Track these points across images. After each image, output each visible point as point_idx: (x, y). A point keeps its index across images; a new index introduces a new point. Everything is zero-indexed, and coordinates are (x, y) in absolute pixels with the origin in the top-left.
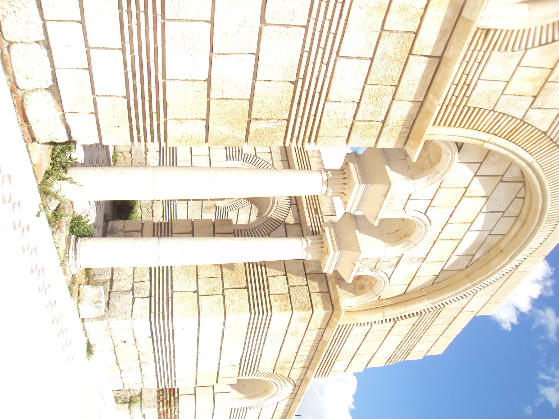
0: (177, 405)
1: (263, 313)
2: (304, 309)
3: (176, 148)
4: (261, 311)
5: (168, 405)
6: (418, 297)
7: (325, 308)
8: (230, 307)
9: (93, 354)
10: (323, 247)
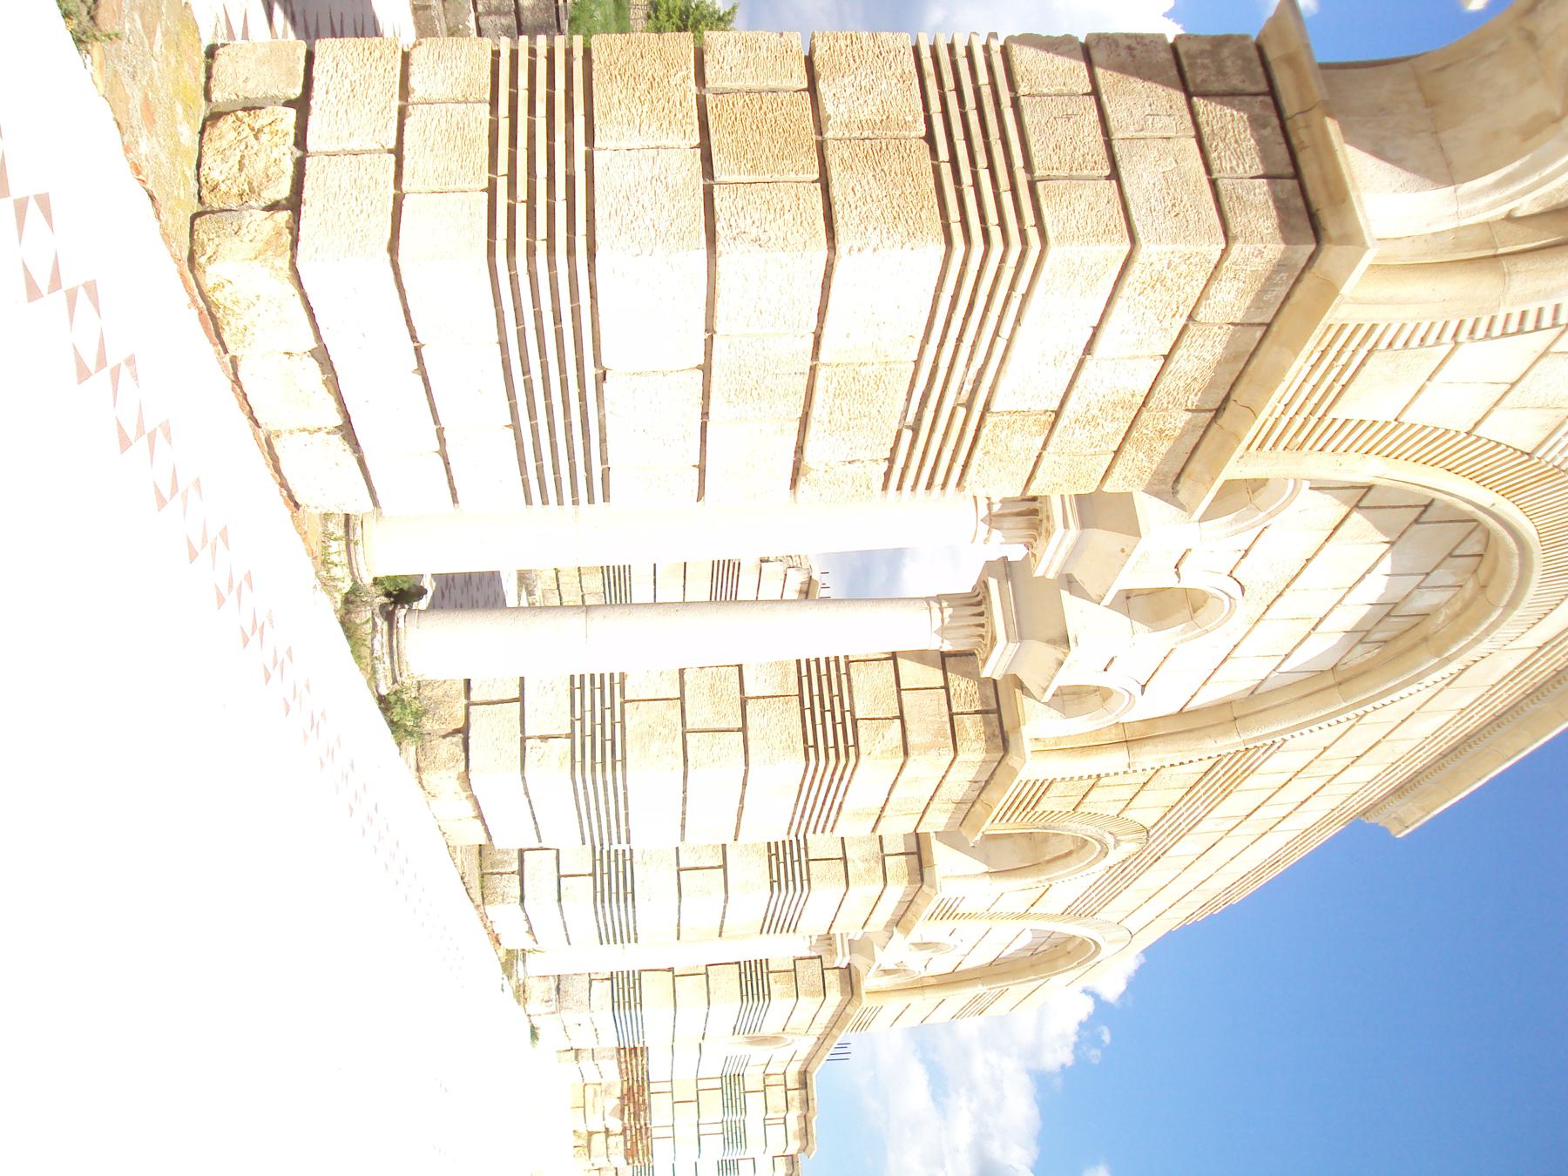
0: (645, 1055)
1: (759, 1000)
2: (812, 994)
3: (630, 566)
4: (756, 997)
5: (633, 1055)
6: (971, 979)
7: (843, 992)
8: (715, 993)
9: (538, 1039)
10: (831, 945)
